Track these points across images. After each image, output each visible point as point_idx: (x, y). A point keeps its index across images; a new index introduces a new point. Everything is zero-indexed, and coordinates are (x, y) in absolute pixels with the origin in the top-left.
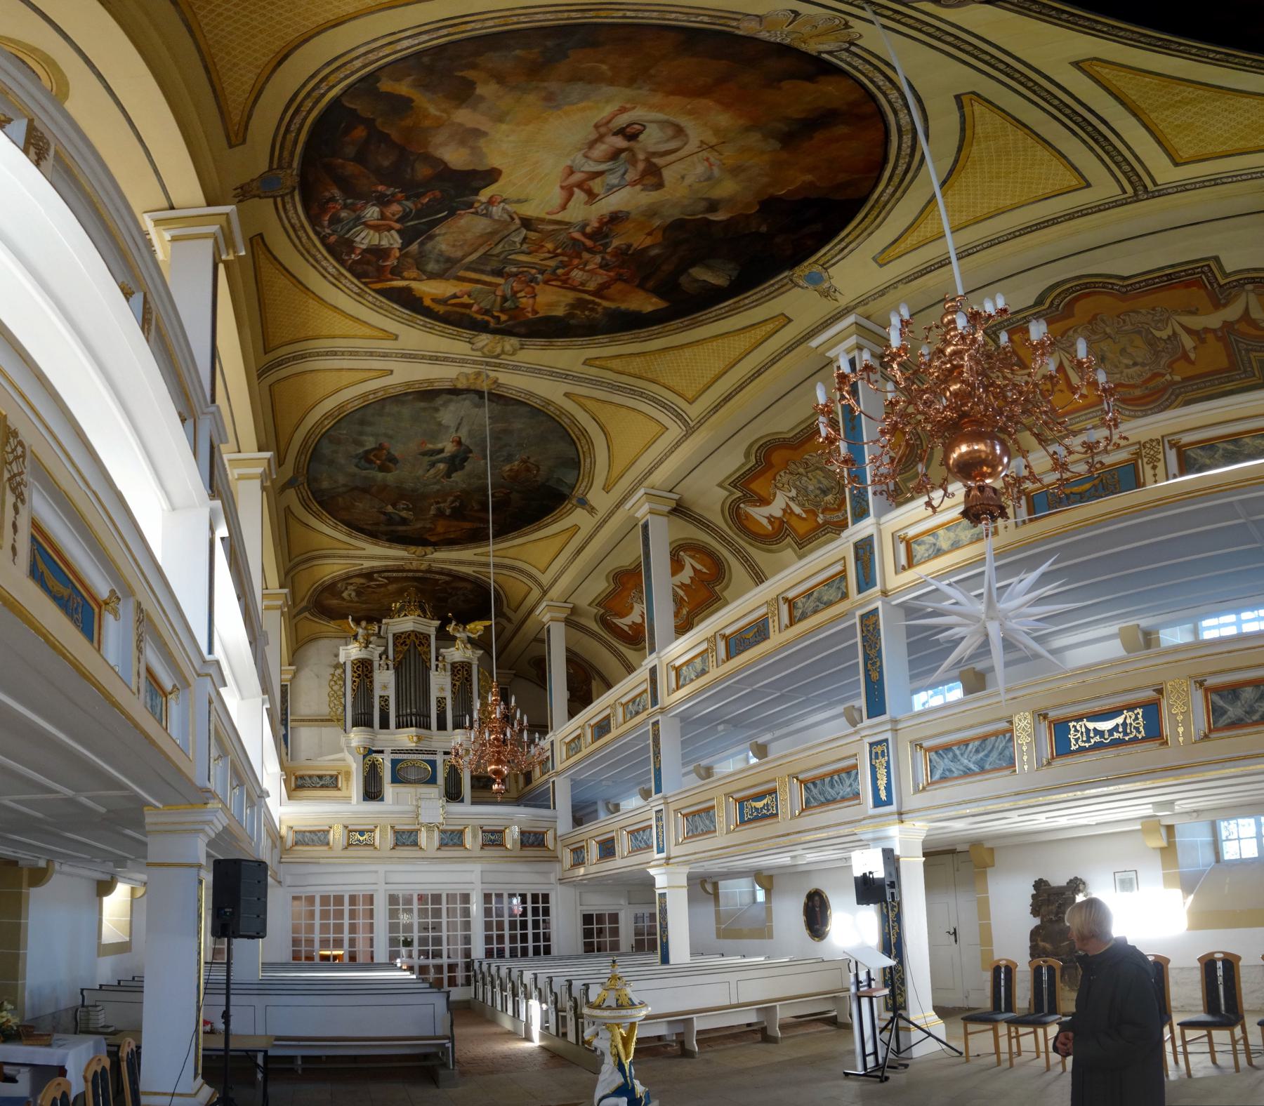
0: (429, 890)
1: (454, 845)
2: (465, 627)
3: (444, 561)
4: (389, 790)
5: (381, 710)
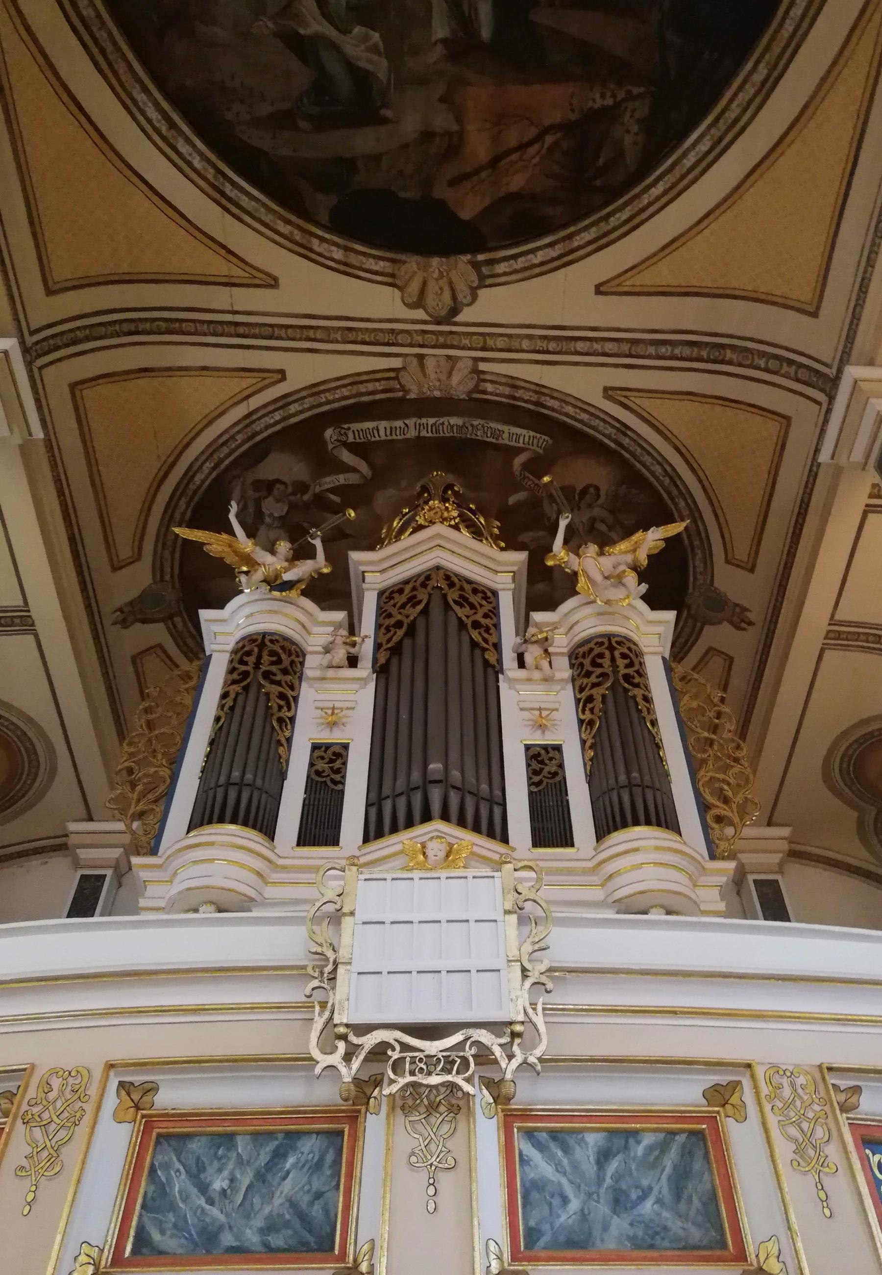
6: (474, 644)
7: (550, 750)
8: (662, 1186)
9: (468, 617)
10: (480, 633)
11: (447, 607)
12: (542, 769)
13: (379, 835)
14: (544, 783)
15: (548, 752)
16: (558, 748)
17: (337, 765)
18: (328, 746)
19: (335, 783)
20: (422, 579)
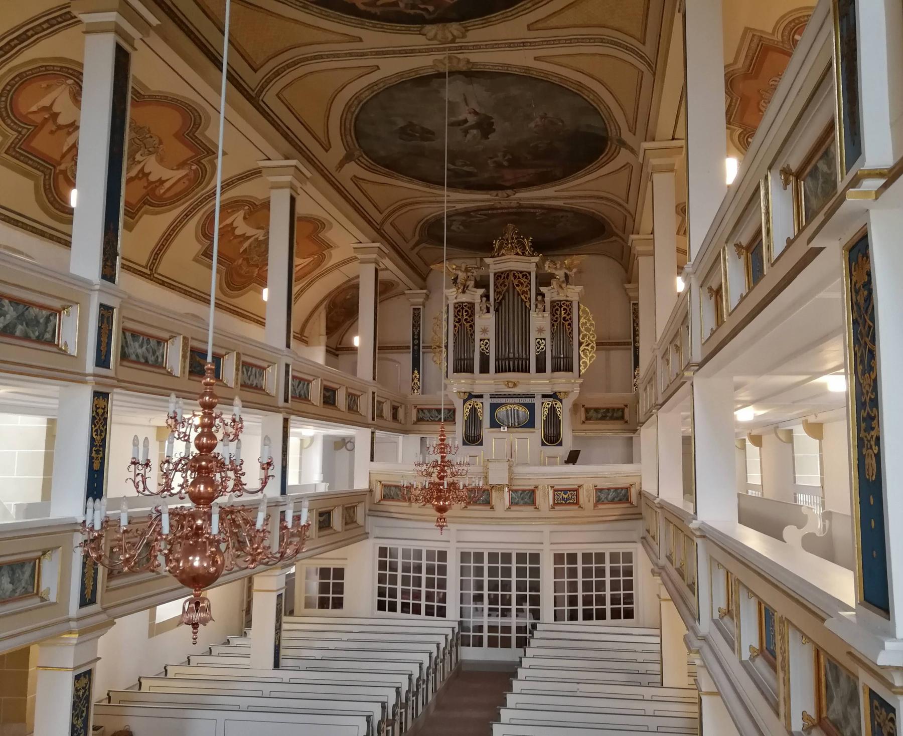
0: (500, 549)
1: (525, 504)
3: (528, 199)
4: (487, 432)
5: (482, 354)
6: (522, 300)
8: (528, 497)
11: (514, 288)
13: (499, 372)
17: (487, 346)
18: (484, 340)
19: (487, 353)
20: (506, 274)
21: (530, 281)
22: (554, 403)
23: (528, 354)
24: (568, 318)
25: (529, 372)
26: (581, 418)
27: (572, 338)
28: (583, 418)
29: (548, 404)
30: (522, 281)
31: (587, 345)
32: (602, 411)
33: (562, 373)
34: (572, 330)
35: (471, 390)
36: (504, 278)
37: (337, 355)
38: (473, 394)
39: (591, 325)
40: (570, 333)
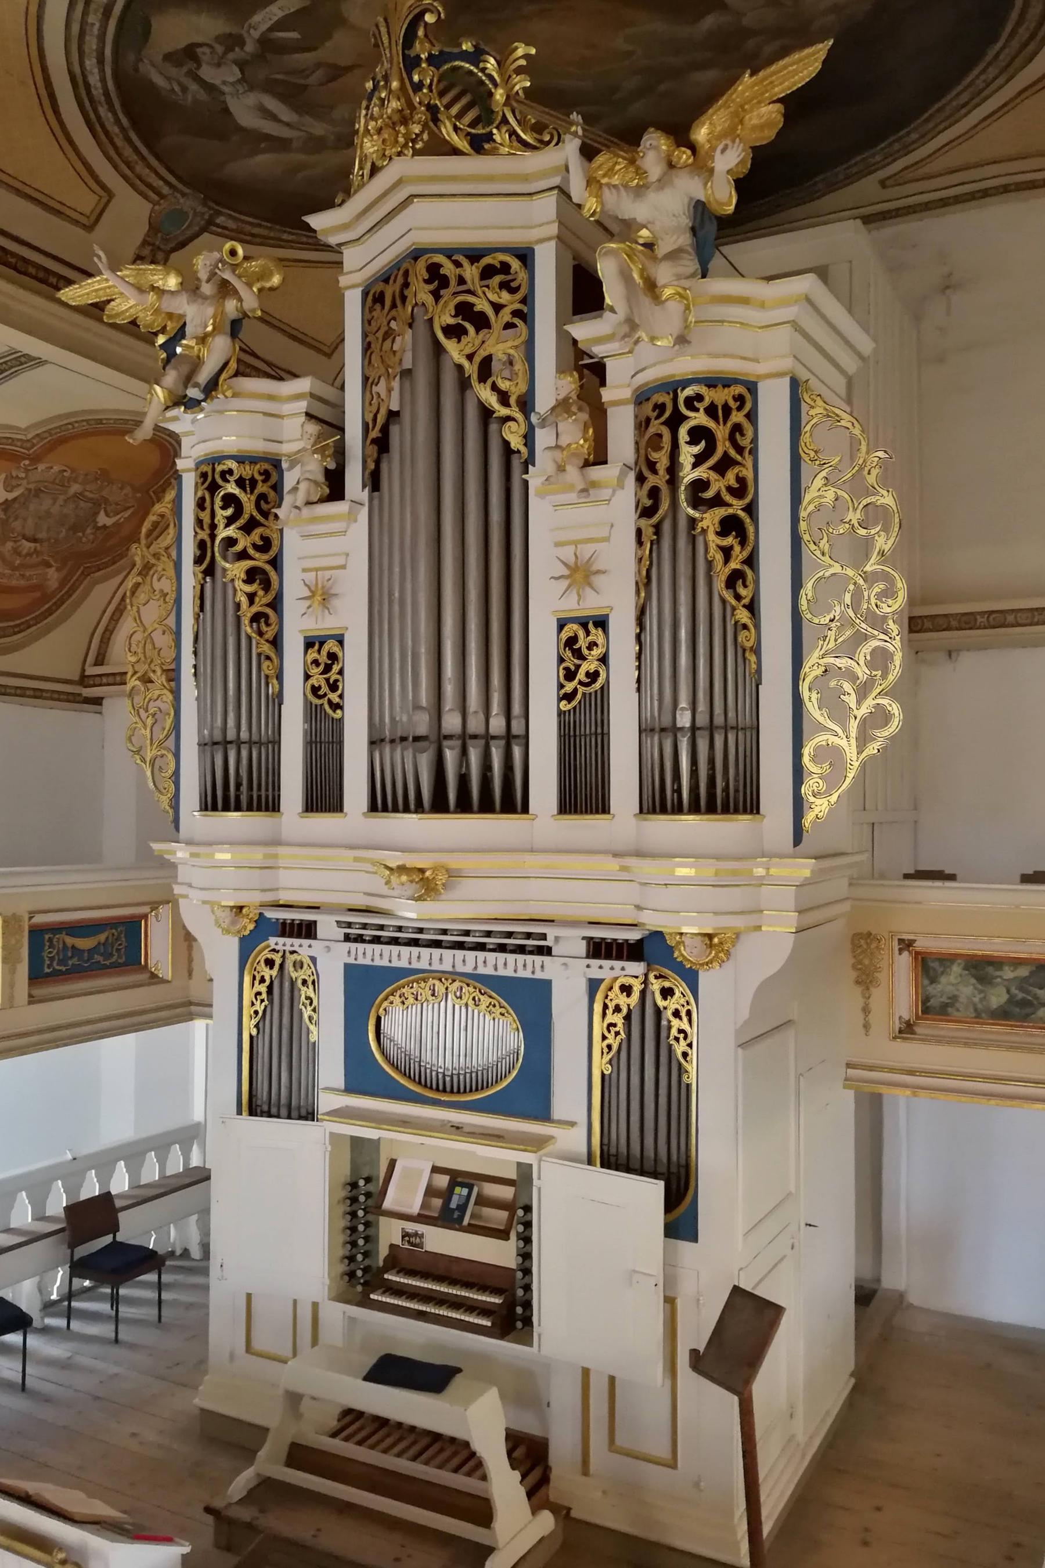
2: (681, 136)
6: (486, 413)
7: (591, 626)
9: (470, 357)
10: (494, 387)
12: (578, 667)
14: (579, 696)
15: (588, 633)
16: (602, 623)
17: (333, 676)
20: (400, 280)
21: (528, 300)
22: (656, 986)
23: (517, 708)
24: (718, 485)
25: (525, 810)
26: (891, 1001)
27: (752, 607)
28: (905, 1004)
29: (627, 990)
30: (482, 305)
31: (850, 649)
32: (1008, 973)
33: (690, 820)
34: (751, 561)
35: (257, 898)
36: (394, 306)
37: (98, 701)
38: (271, 914)
39: (874, 515)
40: (734, 579)
